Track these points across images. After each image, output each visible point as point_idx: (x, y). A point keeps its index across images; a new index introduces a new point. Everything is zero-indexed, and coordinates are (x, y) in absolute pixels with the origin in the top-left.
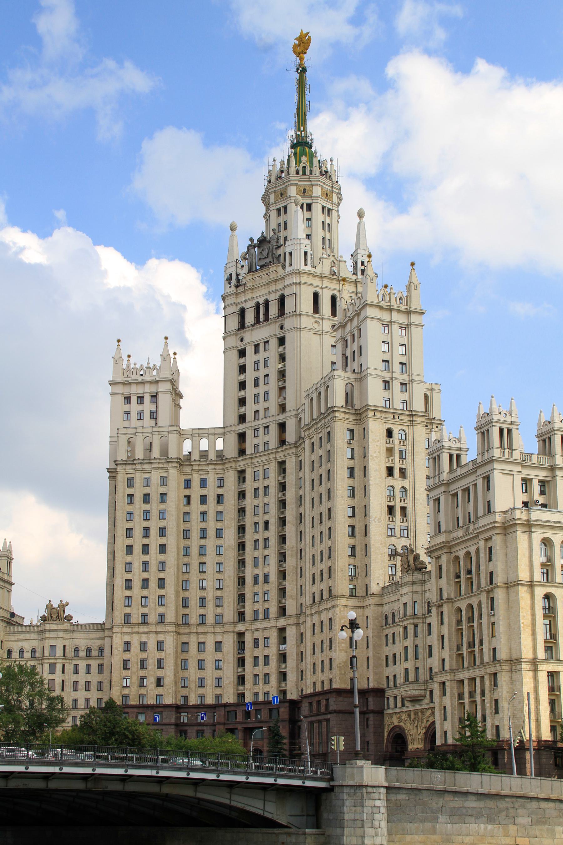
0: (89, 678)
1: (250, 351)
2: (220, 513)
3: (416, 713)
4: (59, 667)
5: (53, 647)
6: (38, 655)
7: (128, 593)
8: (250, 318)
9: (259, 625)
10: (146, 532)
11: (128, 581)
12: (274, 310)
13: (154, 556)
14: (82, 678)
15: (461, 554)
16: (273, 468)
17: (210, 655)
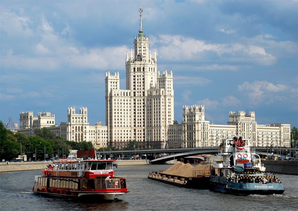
0: (105, 136)
1: (136, 76)
2: (130, 106)
3: (176, 145)
4: (100, 134)
5: (99, 130)
6: (95, 131)
7: (115, 121)
8: (136, 70)
9: (139, 128)
10: (118, 110)
11: (115, 119)
12: (142, 70)
13: (120, 115)
14: (103, 136)
15: (189, 125)
16: (142, 100)
17: (129, 133)
